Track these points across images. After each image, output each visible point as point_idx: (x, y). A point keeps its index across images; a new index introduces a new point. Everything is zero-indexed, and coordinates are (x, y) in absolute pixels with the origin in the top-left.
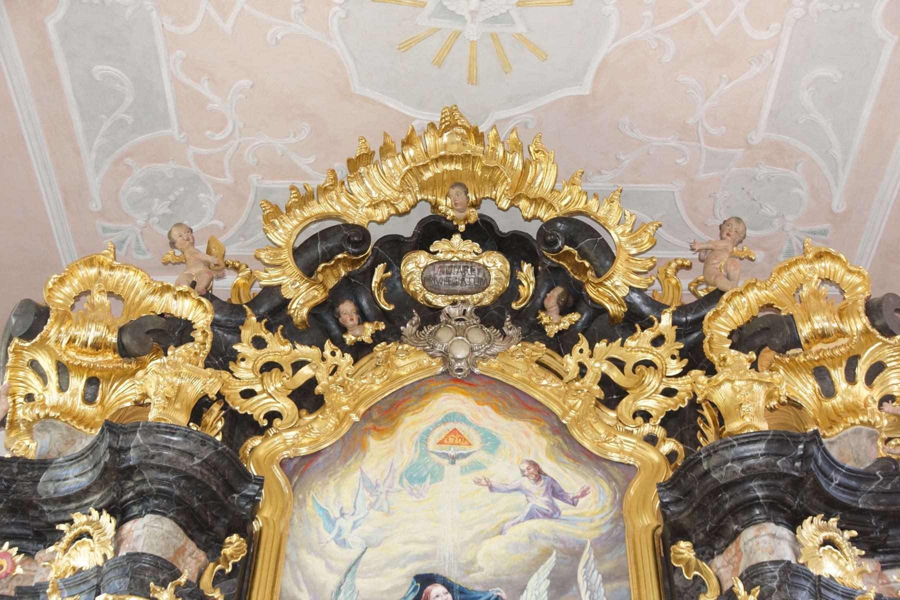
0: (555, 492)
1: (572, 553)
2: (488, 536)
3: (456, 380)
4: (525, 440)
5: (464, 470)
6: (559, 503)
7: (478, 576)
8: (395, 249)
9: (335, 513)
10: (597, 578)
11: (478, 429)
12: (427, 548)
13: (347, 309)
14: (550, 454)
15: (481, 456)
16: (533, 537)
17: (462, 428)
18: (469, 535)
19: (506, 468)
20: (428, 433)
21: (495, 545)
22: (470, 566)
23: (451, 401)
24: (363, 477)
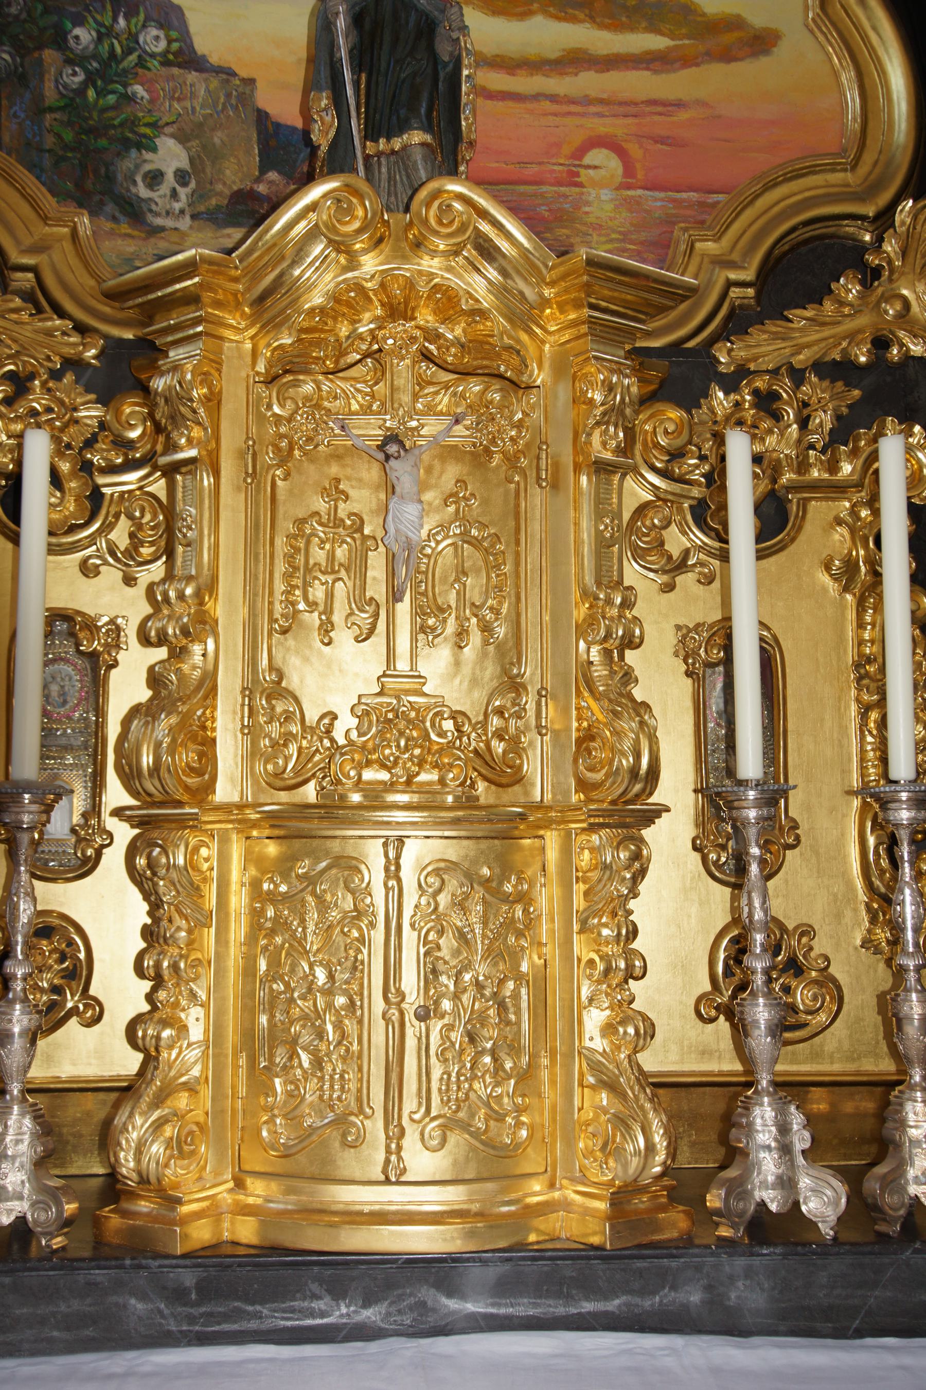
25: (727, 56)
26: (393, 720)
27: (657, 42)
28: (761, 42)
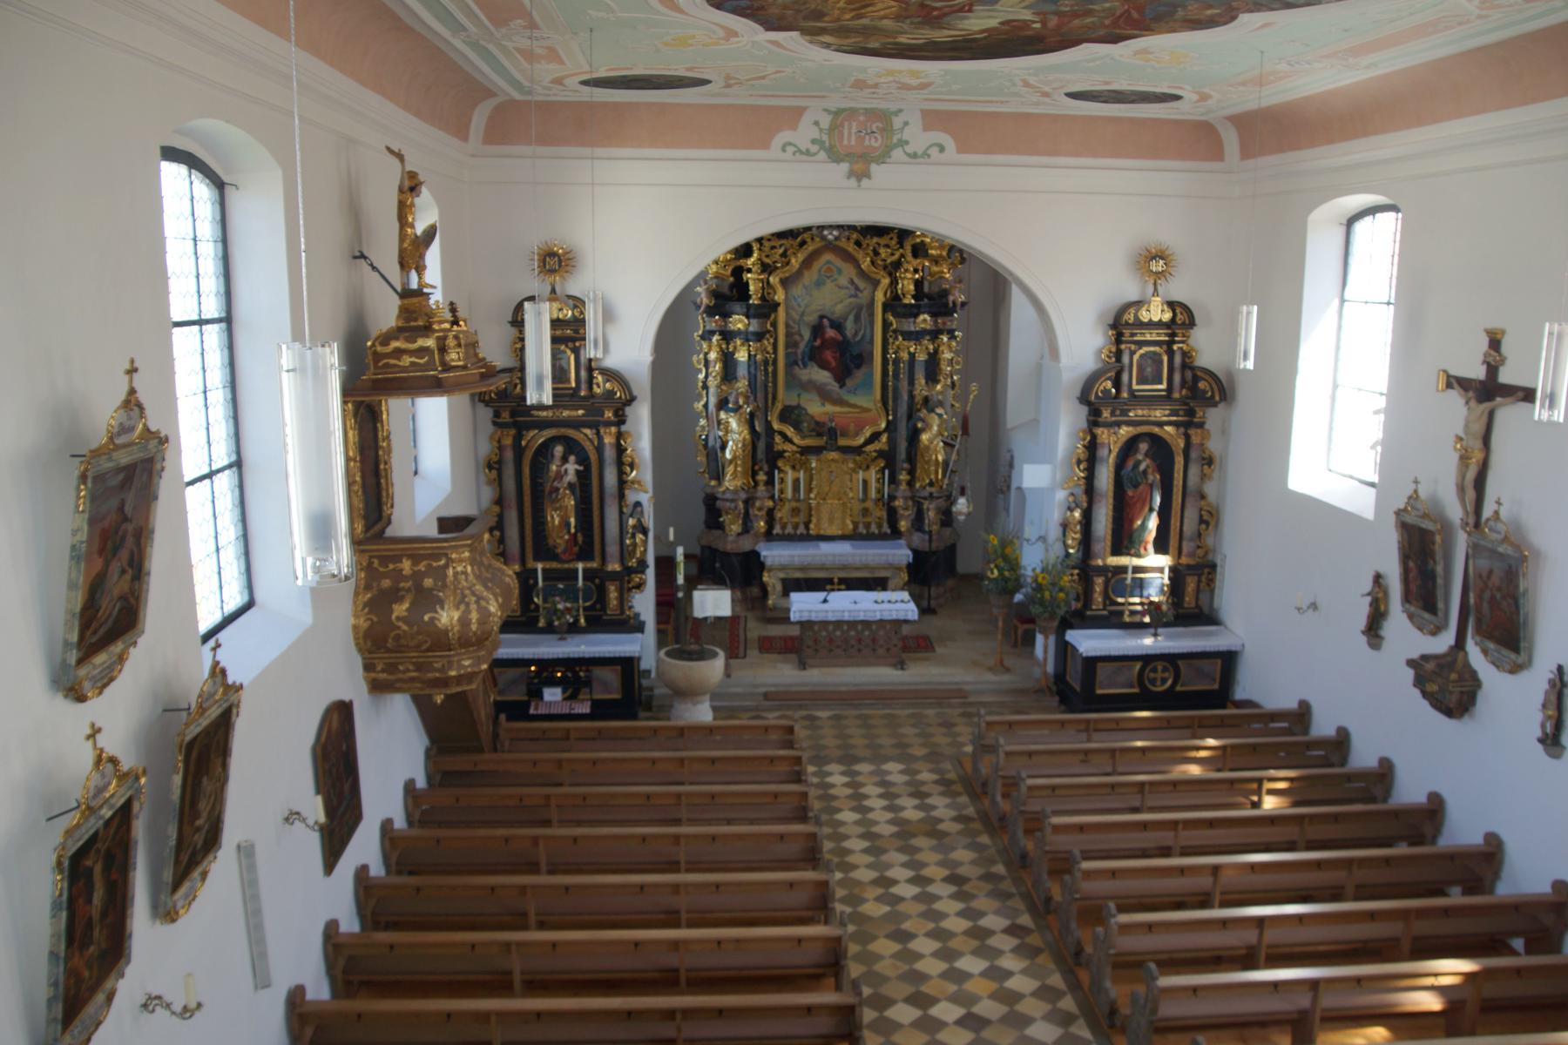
0: (857, 288)
1: (860, 308)
4: (849, 271)
19: (843, 281)
23: (828, 257)
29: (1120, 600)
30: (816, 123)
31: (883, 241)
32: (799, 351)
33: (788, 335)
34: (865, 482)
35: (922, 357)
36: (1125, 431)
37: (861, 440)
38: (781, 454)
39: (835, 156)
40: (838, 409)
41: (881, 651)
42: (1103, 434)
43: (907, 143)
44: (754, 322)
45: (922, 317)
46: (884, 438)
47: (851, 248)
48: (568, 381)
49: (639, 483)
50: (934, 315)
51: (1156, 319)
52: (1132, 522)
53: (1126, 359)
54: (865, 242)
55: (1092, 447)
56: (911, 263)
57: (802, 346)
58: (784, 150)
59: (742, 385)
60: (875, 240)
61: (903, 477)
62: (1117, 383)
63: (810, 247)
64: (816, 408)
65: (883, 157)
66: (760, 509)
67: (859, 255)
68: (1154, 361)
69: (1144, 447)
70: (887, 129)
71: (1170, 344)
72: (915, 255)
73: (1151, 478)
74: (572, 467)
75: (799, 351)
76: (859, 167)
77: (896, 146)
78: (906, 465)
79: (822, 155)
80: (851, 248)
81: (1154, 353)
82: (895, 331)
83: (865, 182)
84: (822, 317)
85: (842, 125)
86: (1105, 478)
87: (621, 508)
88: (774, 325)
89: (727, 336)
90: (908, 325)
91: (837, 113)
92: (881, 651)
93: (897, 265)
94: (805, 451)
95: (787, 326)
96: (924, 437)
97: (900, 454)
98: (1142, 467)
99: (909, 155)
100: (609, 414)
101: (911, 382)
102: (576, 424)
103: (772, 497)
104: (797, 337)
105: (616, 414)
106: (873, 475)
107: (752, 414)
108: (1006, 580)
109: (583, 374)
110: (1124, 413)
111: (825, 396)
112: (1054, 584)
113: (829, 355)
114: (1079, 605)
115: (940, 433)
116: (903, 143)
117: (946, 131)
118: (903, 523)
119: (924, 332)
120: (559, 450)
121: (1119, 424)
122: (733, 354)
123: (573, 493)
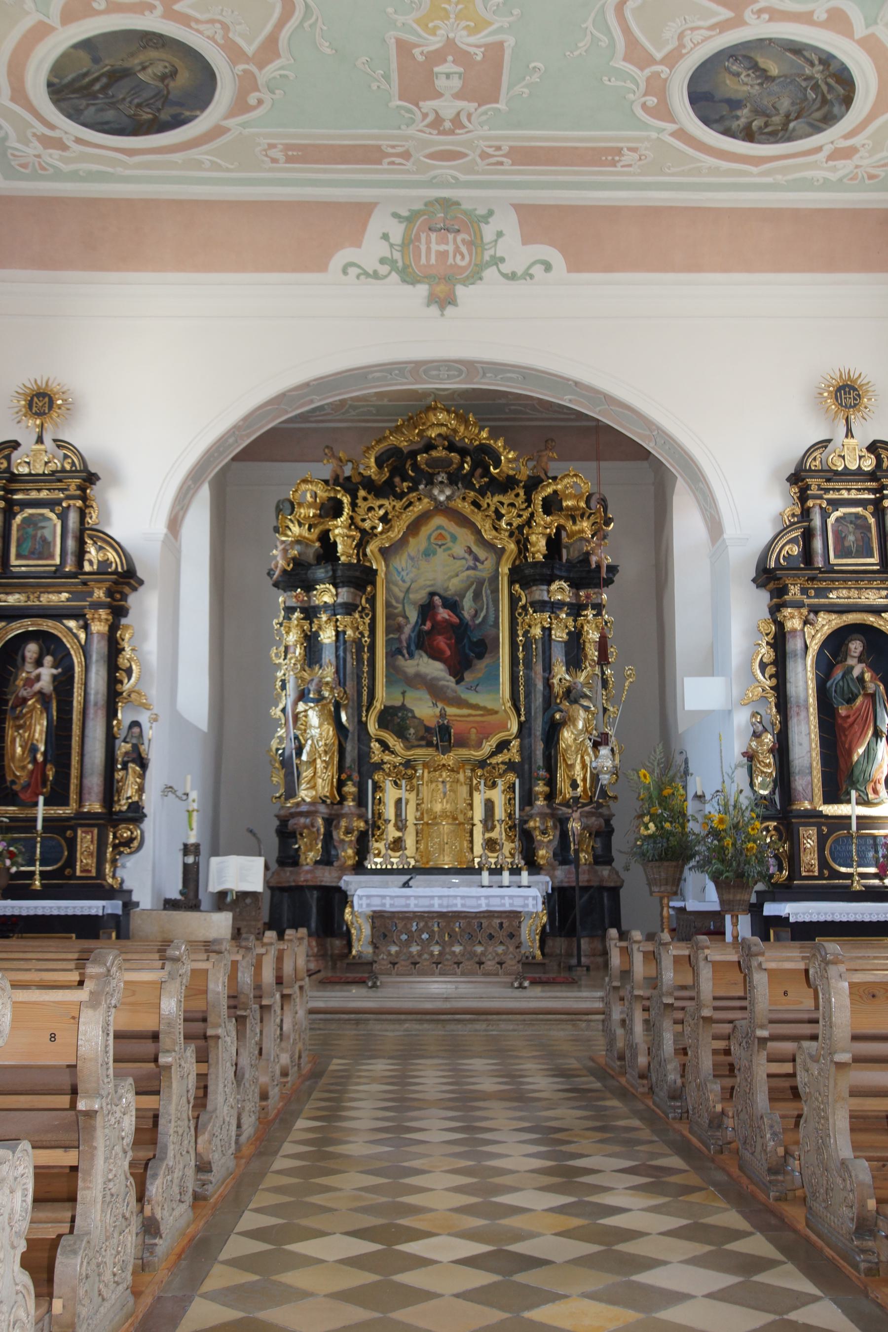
0: (476, 559)
1: (480, 583)
2: (452, 577)
3: (441, 510)
4: (465, 537)
5: (445, 550)
6: (478, 564)
7: (449, 593)
8: (413, 454)
9: (400, 569)
10: (489, 592)
11: (450, 533)
12: (432, 582)
13: (397, 480)
14: (475, 543)
15: (450, 544)
16: (468, 577)
17: (443, 532)
18: (446, 577)
19: (459, 550)
20: (430, 535)
21: (455, 581)
22: (447, 589)
23: (439, 520)
24: (409, 555)
25: (491, 714)
26: (444, 811)
27: (481, 712)
28: (496, 712)
29: (843, 870)
30: (385, 237)
31: (506, 500)
32: (404, 637)
33: (389, 617)
34: (489, 806)
35: (559, 635)
36: (827, 623)
37: (488, 746)
38: (379, 766)
39: (409, 277)
40: (451, 711)
41: (490, 965)
42: (794, 623)
43: (502, 260)
44: (343, 591)
45: (554, 586)
46: (515, 743)
47: (466, 508)
48: (52, 557)
49: (139, 693)
50: (576, 585)
51: (853, 467)
52: (850, 753)
53: (817, 521)
54: (484, 503)
55: (780, 642)
56: (542, 519)
57: (407, 630)
58: (345, 272)
59: (328, 673)
60: (497, 498)
61: (540, 788)
62: (807, 554)
63: (418, 508)
64: (425, 710)
65: (474, 276)
66: (348, 832)
67: (477, 518)
68: (857, 527)
69: (856, 647)
70: (476, 244)
71: (877, 504)
72: (547, 511)
73: (871, 687)
74: (47, 673)
75: (404, 637)
76: (441, 289)
77: (488, 265)
78: (542, 773)
79: (394, 276)
80: (466, 508)
81: (857, 516)
82: (524, 608)
83: (450, 310)
84: (432, 594)
85: (418, 239)
86: (803, 679)
87: (109, 728)
88: (372, 600)
89: (310, 613)
90: (540, 593)
91: (410, 219)
92: (490, 965)
93: (528, 523)
94: (408, 764)
95: (388, 605)
96: (567, 735)
97: (537, 761)
98: (856, 673)
99: (505, 276)
100: (99, 594)
101: (548, 667)
102: (58, 614)
103: (361, 817)
104: (401, 620)
105: (110, 593)
106: (498, 796)
107: (338, 706)
108: (671, 833)
109: (71, 544)
110: (822, 593)
111: (436, 692)
112: (736, 826)
113: (441, 642)
114: (785, 873)
115: (586, 730)
116: (497, 261)
117: (552, 244)
118: (542, 852)
119: (560, 605)
120: (32, 649)
121: (815, 610)
122: (316, 635)
123: (46, 708)
